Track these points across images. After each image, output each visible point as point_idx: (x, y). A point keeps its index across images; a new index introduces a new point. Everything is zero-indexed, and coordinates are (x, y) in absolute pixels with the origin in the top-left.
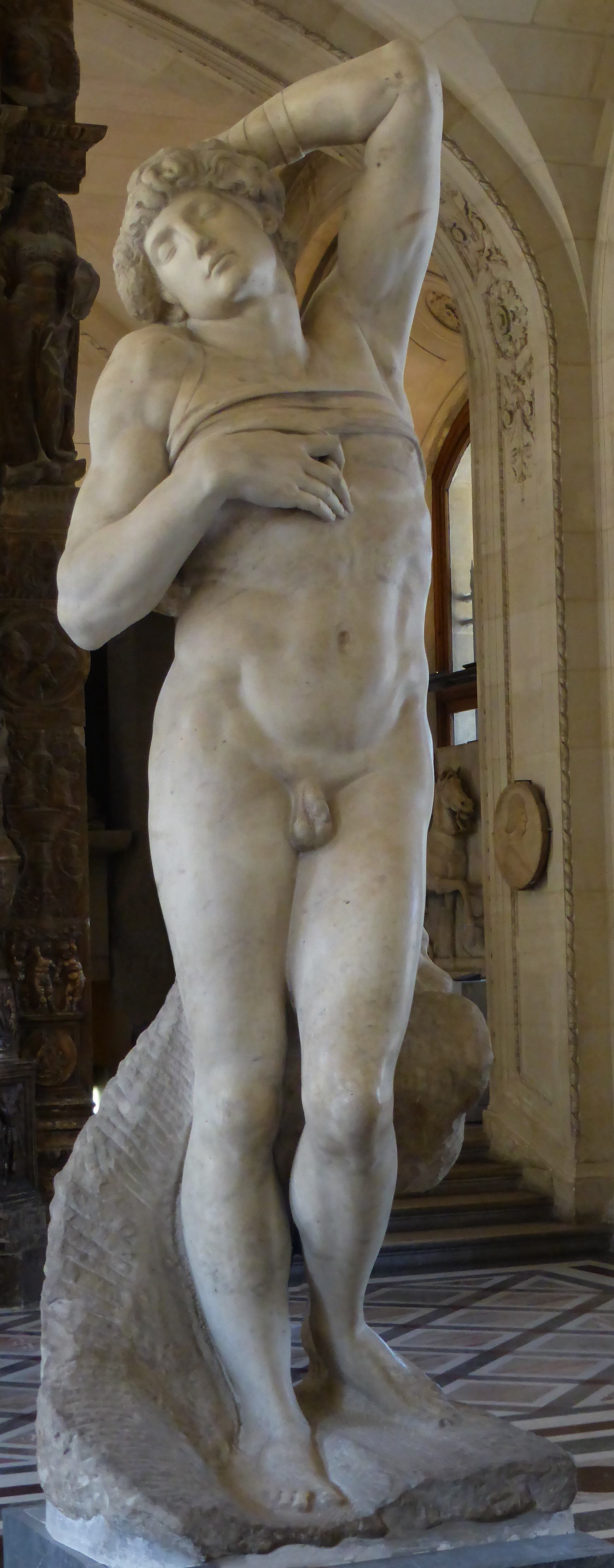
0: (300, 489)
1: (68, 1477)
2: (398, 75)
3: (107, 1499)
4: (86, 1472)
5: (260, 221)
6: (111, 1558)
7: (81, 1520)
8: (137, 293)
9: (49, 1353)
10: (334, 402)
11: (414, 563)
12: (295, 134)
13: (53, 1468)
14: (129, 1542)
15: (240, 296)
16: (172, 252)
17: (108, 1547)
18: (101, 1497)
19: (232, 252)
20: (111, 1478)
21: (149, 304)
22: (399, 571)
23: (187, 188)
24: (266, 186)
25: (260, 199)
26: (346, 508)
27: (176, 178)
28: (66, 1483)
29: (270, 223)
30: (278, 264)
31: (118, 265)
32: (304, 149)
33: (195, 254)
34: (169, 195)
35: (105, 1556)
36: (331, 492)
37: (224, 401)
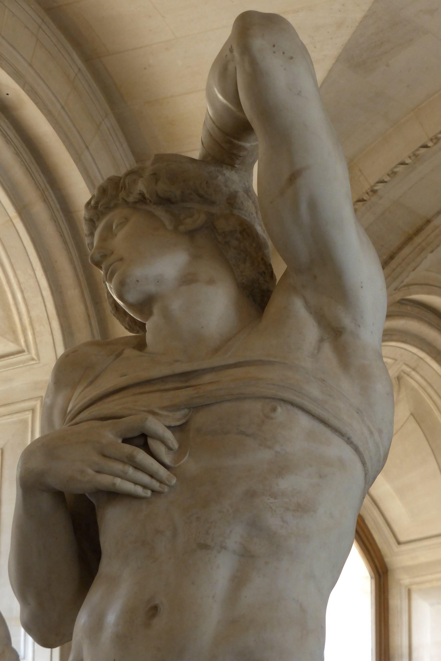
0: (98, 472)
2: (231, 50)
5: (167, 223)
8: (113, 312)
10: (208, 378)
11: (256, 526)
12: (219, 128)
15: (132, 297)
19: (121, 259)
21: (128, 319)
22: (235, 536)
23: (108, 208)
24: (162, 187)
25: (165, 201)
26: (161, 482)
27: (97, 203)
29: (189, 221)
30: (195, 257)
32: (239, 139)
34: (95, 220)
36: (131, 471)
37: (86, 400)
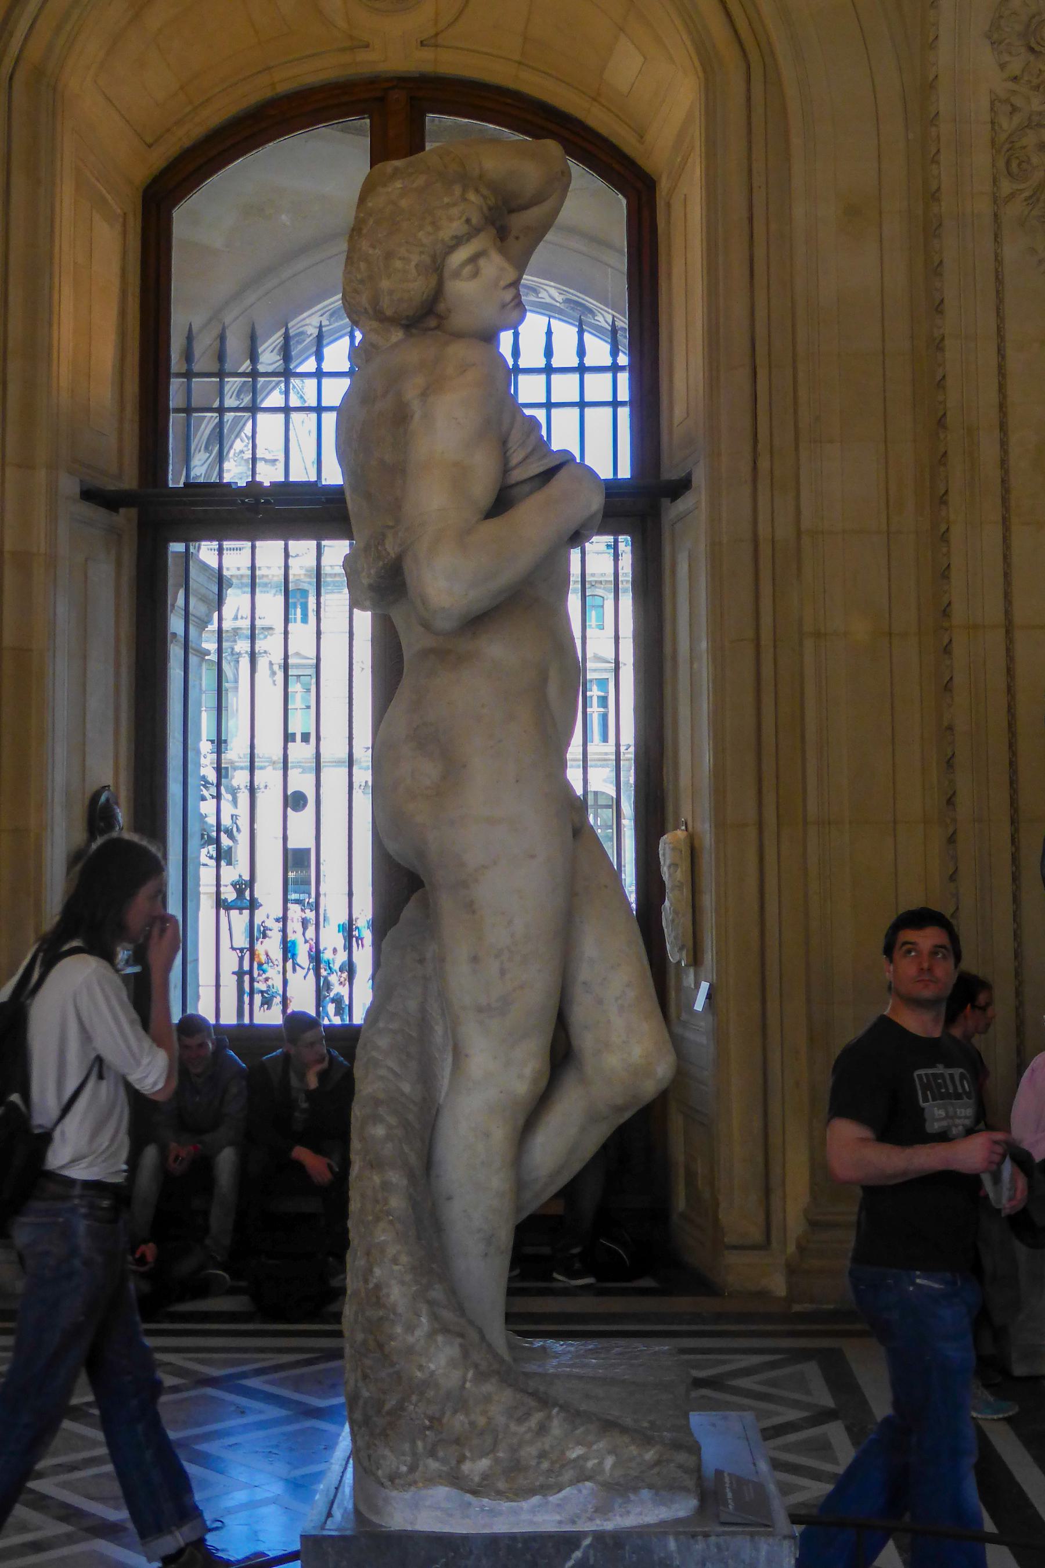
1: (542, 1455)
3: (609, 1462)
4: (579, 1443)
6: (608, 1520)
7: (536, 1500)
9: (459, 1340)
13: (501, 1454)
14: (632, 1497)
16: (476, 274)
17: (603, 1510)
18: (601, 1463)
20: (626, 1439)
28: (539, 1463)
31: (417, 266)
33: (502, 283)
35: (598, 1522)
